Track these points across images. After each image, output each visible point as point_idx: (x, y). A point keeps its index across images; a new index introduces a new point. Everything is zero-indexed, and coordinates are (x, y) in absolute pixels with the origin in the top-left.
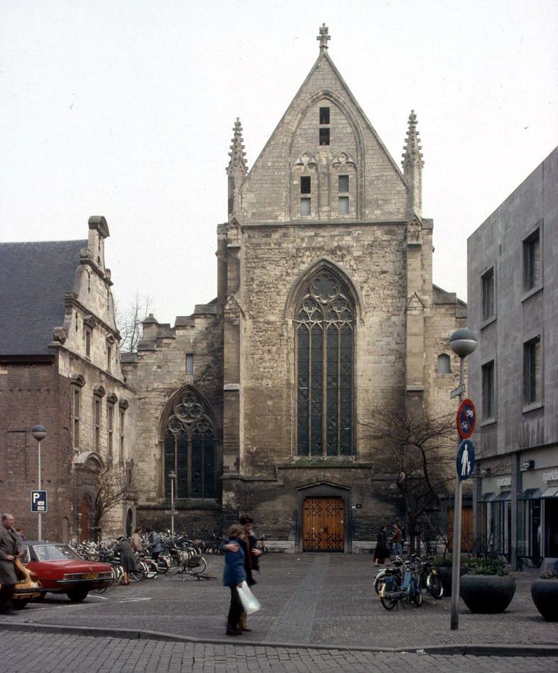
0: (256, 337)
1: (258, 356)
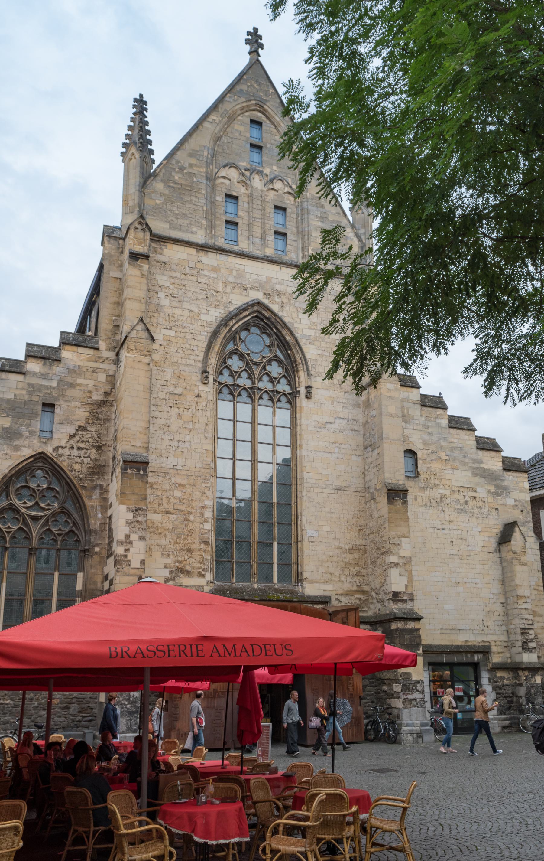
0: (160, 393)
1: (163, 422)
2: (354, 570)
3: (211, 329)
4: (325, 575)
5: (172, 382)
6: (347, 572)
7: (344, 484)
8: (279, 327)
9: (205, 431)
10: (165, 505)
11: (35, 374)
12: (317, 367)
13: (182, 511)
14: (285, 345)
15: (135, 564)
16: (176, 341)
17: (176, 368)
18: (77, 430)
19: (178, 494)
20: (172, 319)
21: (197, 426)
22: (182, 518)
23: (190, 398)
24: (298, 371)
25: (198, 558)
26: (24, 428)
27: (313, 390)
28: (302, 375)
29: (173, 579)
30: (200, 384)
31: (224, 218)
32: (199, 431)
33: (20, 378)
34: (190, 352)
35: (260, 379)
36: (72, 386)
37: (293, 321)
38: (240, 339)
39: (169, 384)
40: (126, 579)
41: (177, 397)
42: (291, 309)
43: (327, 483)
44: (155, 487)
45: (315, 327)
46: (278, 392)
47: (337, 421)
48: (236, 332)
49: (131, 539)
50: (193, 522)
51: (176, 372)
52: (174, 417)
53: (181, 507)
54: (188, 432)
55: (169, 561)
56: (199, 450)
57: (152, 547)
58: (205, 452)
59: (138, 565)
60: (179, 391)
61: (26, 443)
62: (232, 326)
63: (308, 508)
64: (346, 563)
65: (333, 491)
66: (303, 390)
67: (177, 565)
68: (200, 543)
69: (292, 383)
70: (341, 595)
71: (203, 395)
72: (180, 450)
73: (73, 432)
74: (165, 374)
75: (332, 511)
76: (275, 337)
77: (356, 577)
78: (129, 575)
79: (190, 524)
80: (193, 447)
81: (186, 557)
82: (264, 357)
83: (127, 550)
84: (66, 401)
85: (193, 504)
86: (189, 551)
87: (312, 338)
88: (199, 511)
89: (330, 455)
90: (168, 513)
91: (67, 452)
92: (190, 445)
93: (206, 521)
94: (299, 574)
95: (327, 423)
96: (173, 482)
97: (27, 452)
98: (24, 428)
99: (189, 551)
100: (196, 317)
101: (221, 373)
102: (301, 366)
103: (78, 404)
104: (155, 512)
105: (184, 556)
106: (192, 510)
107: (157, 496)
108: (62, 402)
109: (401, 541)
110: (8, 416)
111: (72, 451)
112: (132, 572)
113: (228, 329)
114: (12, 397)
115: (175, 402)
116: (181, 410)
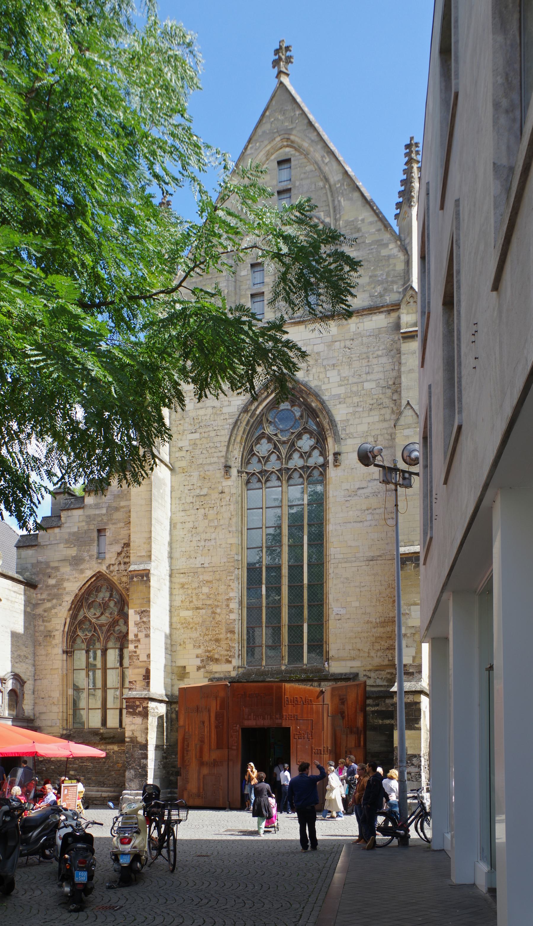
2: (386, 644)
3: (232, 421)
4: (352, 652)
5: (198, 485)
6: (377, 646)
7: (378, 554)
8: (304, 396)
9: (229, 525)
10: (195, 602)
11: (90, 506)
12: (347, 429)
13: (209, 605)
14: (312, 413)
15: (143, 658)
16: (201, 442)
17: (201, 469)
18: (123, 547)
19: (205, 590)
20: (196, 421)
21: (222, 522)
22: (210, 611)
23: (215, 495)
24: (326, 439)
25: (225, 646)
26: (85, 554)
27: (342, 458)
28: (330, 441)
29: (204, 667)
30: (222, 480)
31: (249, 293)
32: (223, 527)
33: (79, 512)
34: (213, 450)
35: (289, 457)
36: (117, 509)
37: (320, 384)
38: (267, 420)
39: (195, 487)
40: (137, 671)
41: (202, 498)
42: (318, 370)
43: (357, 555)
44: (186, 586)
45: (346, 382)
46: (308, 467)
47: (370, 484)
48: (262, 414)
49: (139, 637)
50: (219, 615)
51: (202, 473)
52: (201, 517)
53: (208, 602)
54: (213, 530)
55: (199, 651)
56: (224, 546)
57: (185, 640)
58: (229, 546)
59: (145, 659)
60: (204, 491)
61: (88, 565)
62: (256, 409)
63: (335, 585)
64: (376, 638)
65: (363, 564)
66: (331, 458)
67: (207, 654)
68: (227, 633)
69: (323, 453)
70: (370, 671)
71: (226, 490)
72: (206, 548)
73: (119, 550)
74: (192, 478)
75: (362, 585)
76: (303, 407)
77: (388, 651)
78: (139, 668)
79: (217, 616)
80: (218, 543)
81: (215, 647)
82: (293, 433)
83: (136, 647)
84: (113, 524)
85: (220, 598)
86: (217, 640)
87: (342, 396)
88: (225, 603)
89: (361, 524)
90: (197, 608)
91: (116, 568)
92: (216, 542)
93: (231, 611)
94: (328, 652)
95: (359, 488)
96: (201, 579)
97: (89, 573)
98: (85, 554)
99: (217, 640)
100: (218, 412)
101: (248, 463)
102: (329, 432)
103: (122, 525)
104: (187, 609)
105: (212, 646)
106: (219, 604)
107: (188, 595)
108: (110, 526)
109: (410, 610)
110: (74, 546)
111: (120, 567)
112: (142, 664)
113: (249, 414)
114: (76, 530)
115: (201, 503)
116: (207, 509)
